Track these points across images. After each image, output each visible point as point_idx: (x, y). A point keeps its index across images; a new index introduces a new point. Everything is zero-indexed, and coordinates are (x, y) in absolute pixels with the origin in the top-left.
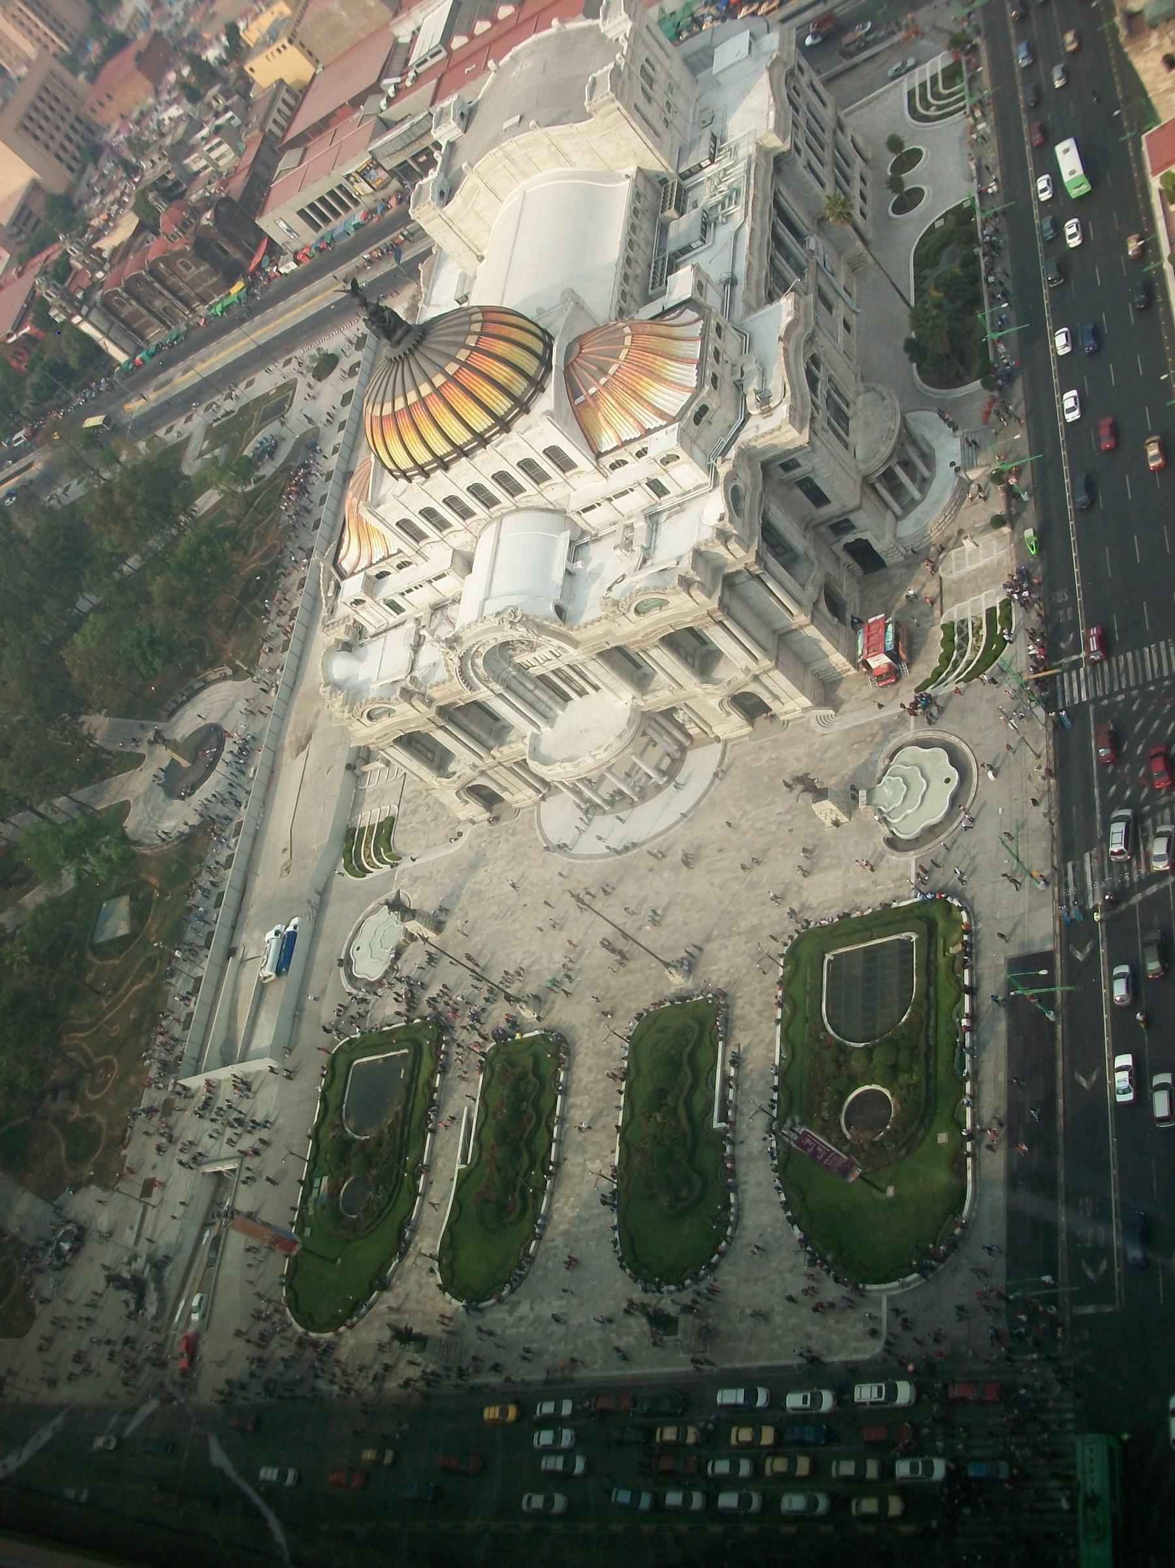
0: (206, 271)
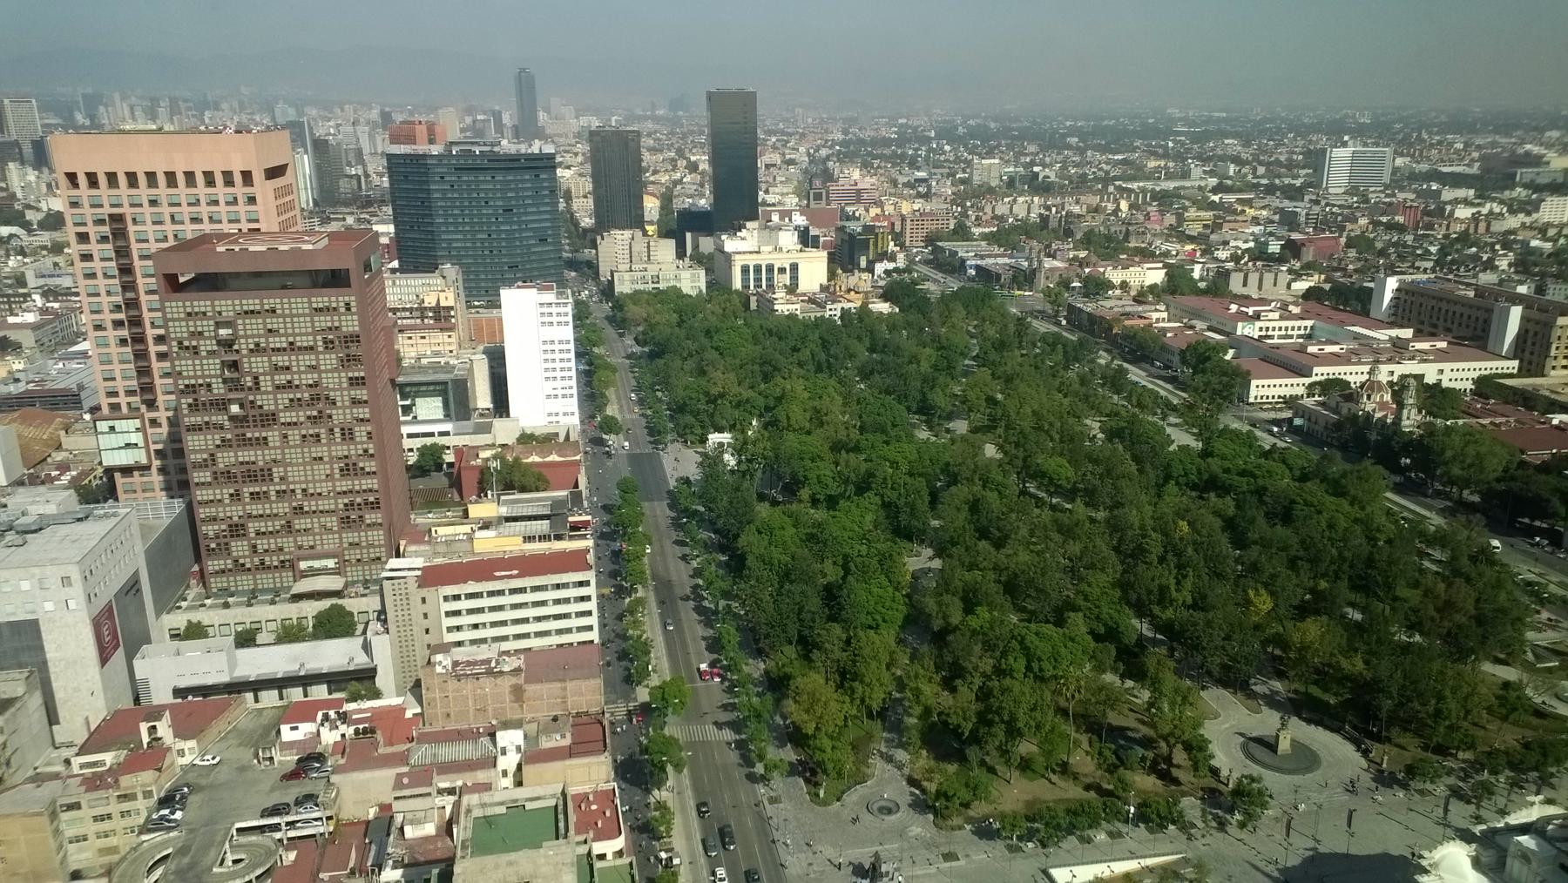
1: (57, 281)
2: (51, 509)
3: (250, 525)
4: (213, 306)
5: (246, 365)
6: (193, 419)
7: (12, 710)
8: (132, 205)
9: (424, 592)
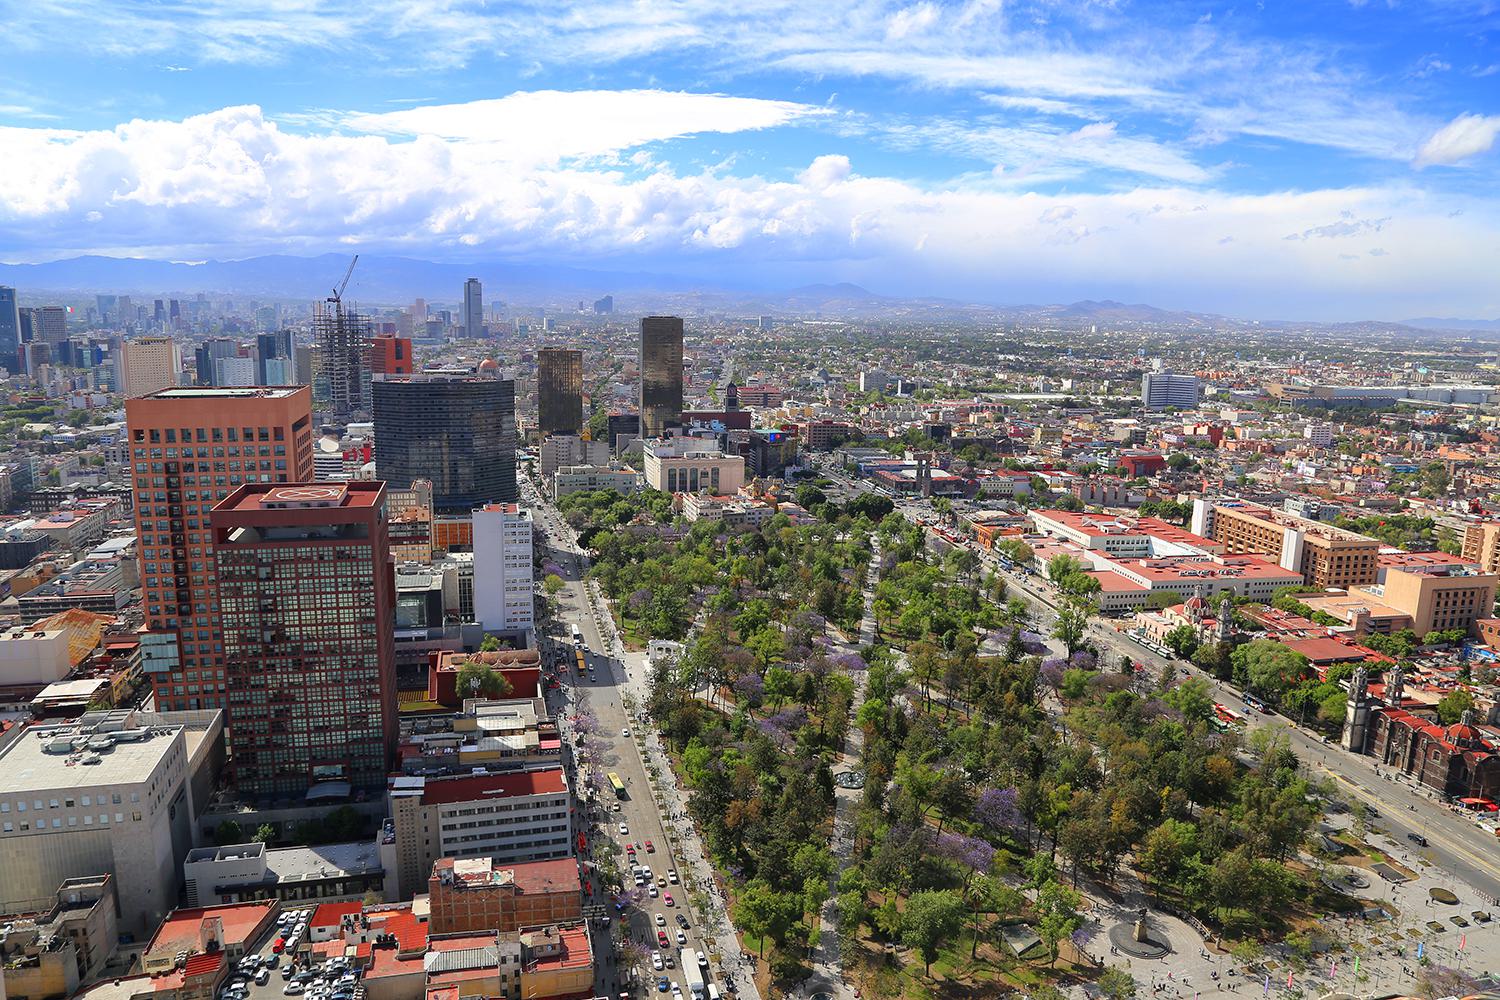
0: (1442, 771)
9: (426, 808)
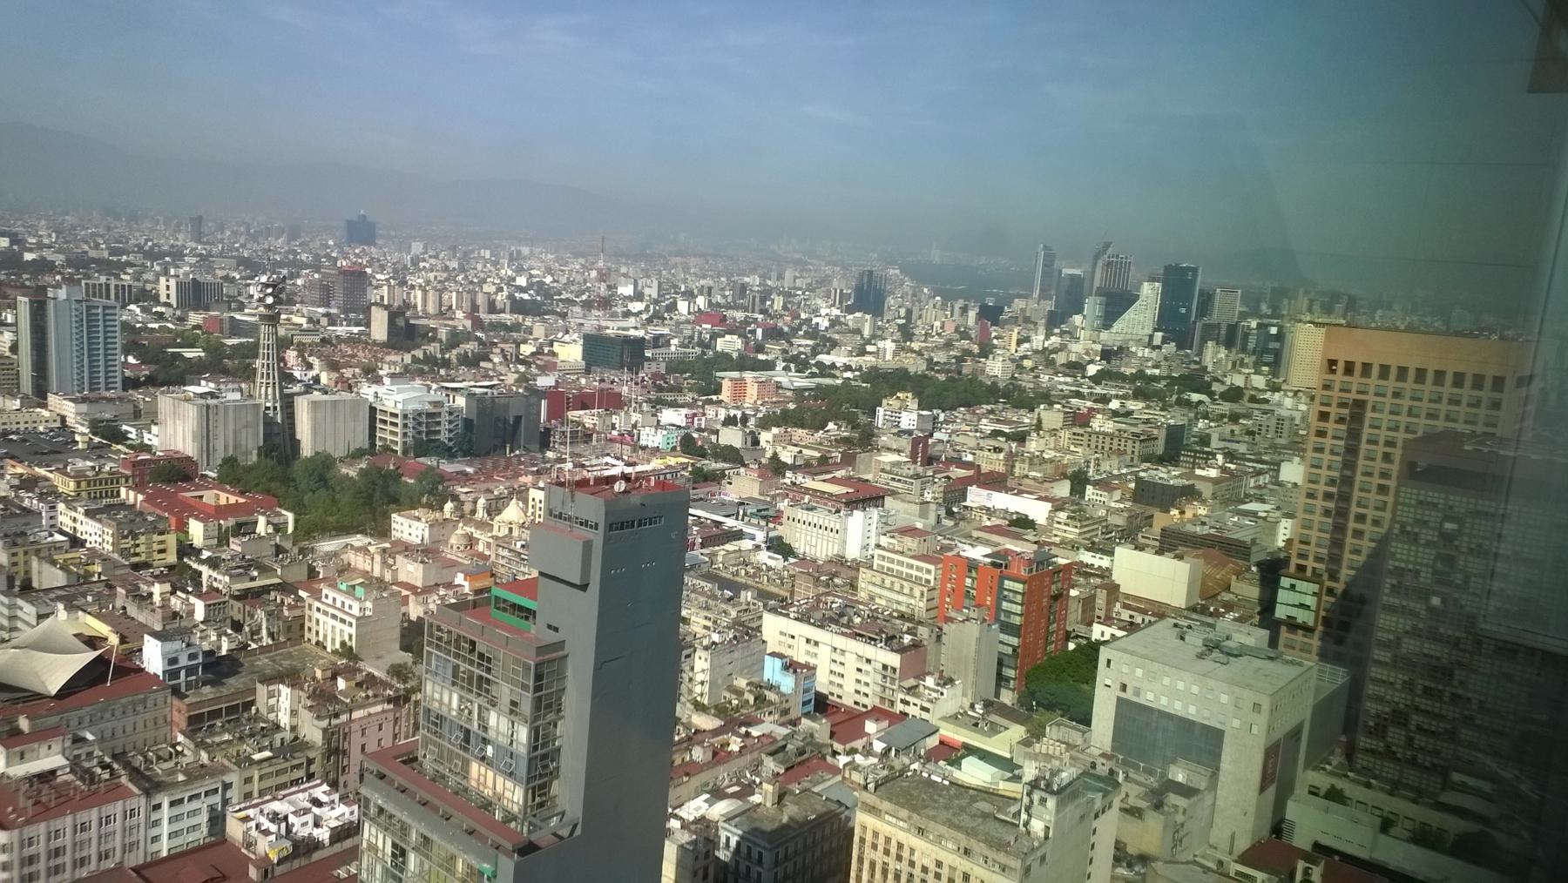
1: (1234, 446)
2: (1250, 641)
3: (1414, 717)
4: (1446, 499)
5: (1461, 563)
6: (1391, 600)
7: (1195, 798)
8: (1377, 394)
